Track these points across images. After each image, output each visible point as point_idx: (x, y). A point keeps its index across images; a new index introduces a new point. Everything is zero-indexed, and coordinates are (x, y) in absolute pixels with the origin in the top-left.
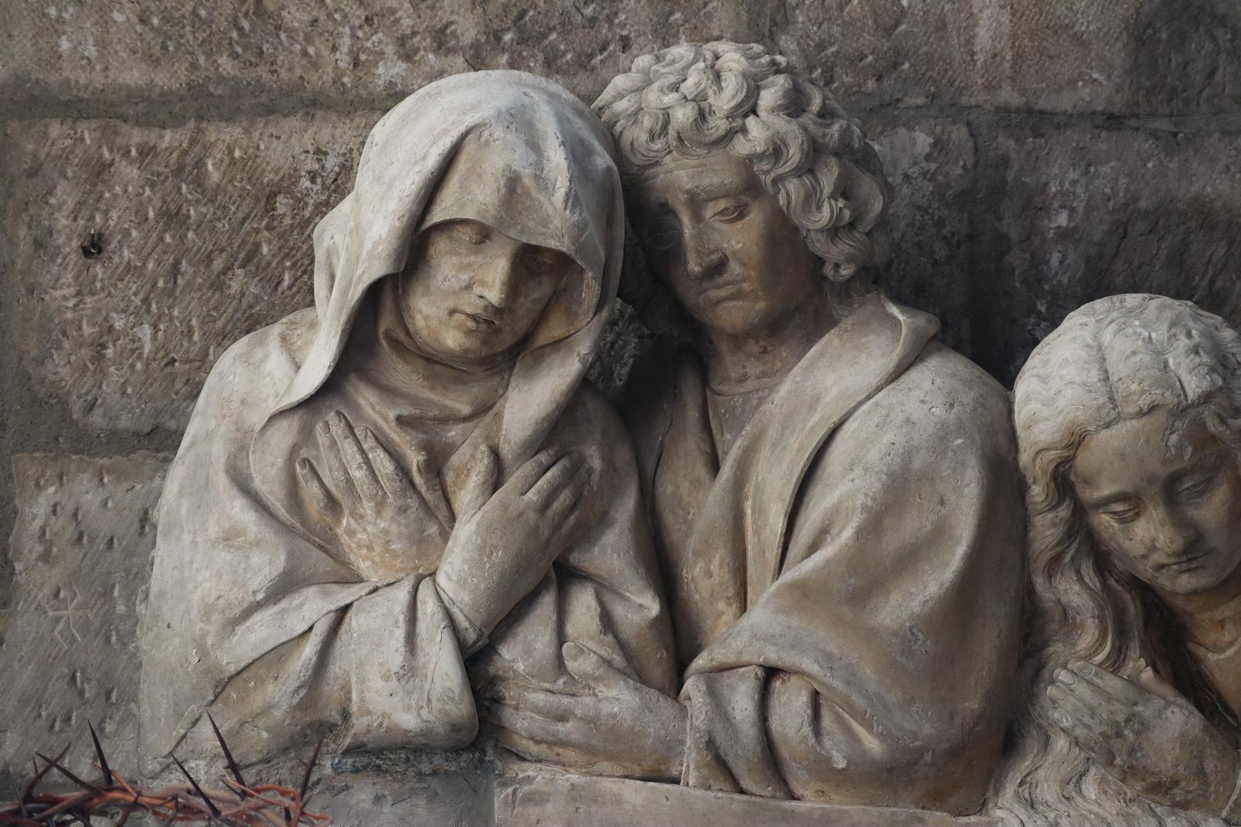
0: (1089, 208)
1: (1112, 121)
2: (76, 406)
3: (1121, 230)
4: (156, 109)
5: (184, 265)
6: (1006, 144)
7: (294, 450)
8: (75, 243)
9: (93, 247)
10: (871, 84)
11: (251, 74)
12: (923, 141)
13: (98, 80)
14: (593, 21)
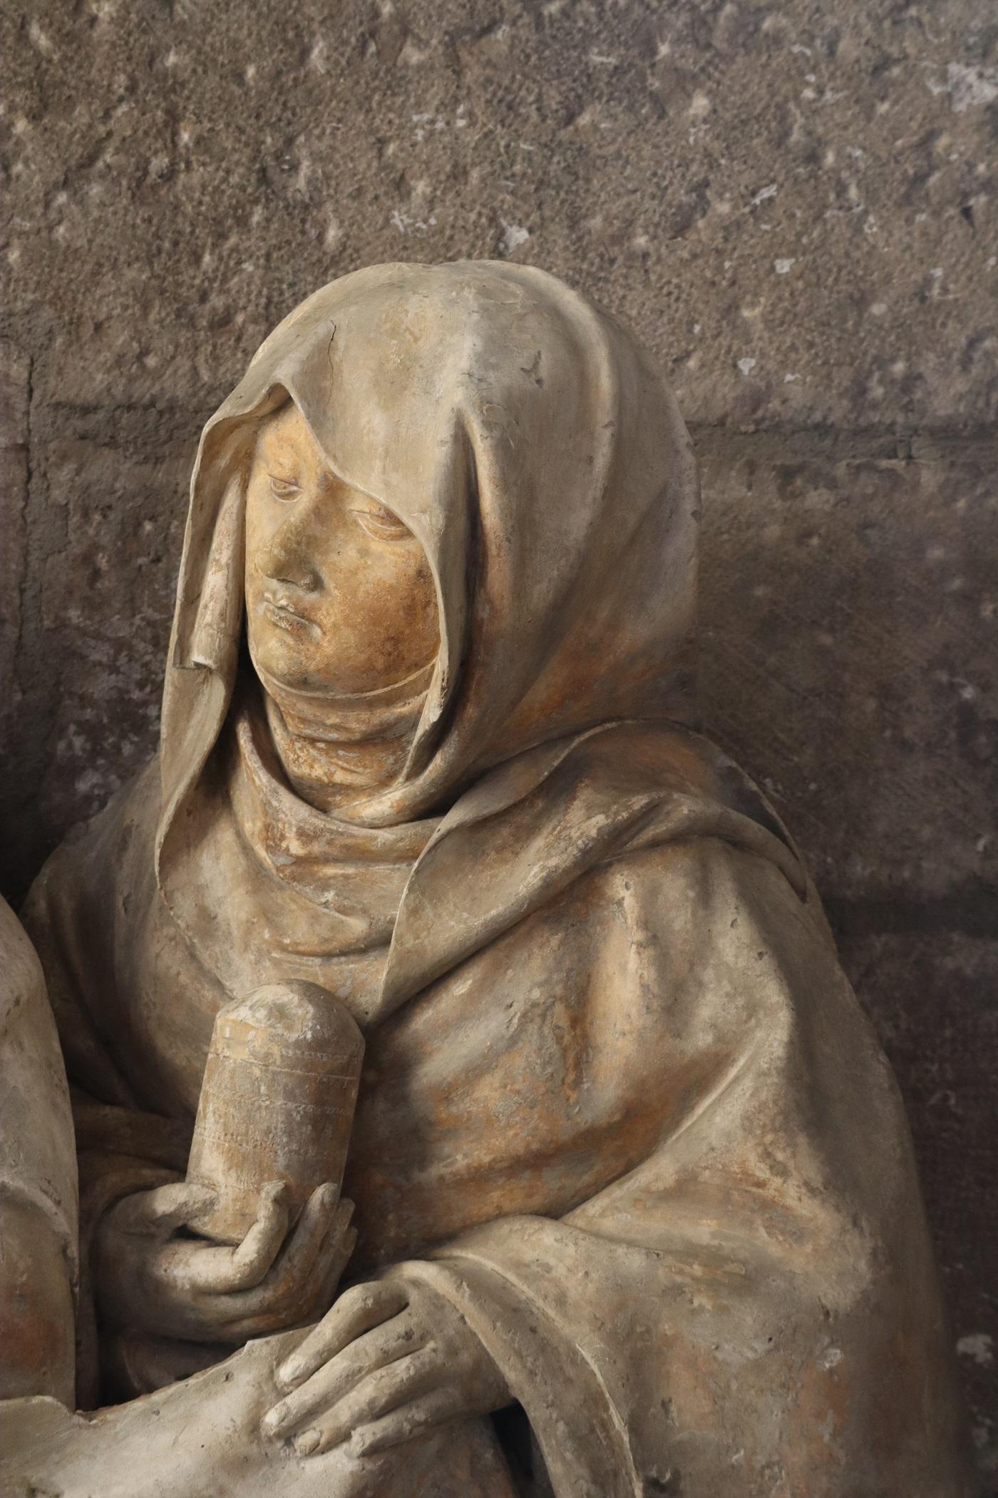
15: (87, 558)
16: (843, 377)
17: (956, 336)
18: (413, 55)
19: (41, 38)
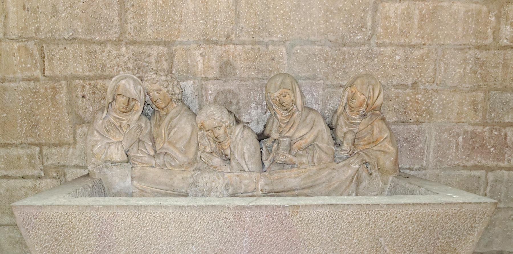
2: (83, 117)
3: (218, 93)
4: (90, 79)
6: (203, 82)
12: (192, 82)
19: (325, 55)
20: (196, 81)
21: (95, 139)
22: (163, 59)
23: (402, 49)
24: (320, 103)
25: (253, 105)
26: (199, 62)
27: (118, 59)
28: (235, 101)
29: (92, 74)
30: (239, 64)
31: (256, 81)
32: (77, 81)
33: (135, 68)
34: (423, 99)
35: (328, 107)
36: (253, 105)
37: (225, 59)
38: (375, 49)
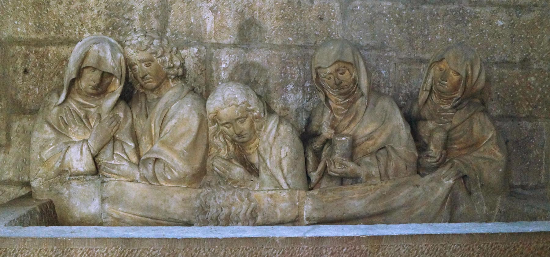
0: (230, 63)
1: (235, 46)
3: (236, 68)
4: (38, 43)
5: (44, 76)
7: (58, 114)
8: (22, 71)
9: (26, 71)
10: (185, 38)
11: (58, 36)
12: (196, 50)
13: (26, 37)
14: (128, 25)
15: (402, 77)
16: (485, 57)
17: (498, 52)
18: (439, 18)
20: (203, 48)
21: (46, 136)
22: (152, 14)
23: (504, 10)
24: (391, 85)
25: (290, 87)
26: (207, 21)
27: (82, 15)
28: (262, 80)
29: (41, 36)
30: (270, 24)
31: (294, 51)
32: (17, 47)
33: (108, 28)
34: (537, 84)
35: (404, 92)
36: (290, 87)
37: (247, 17)
38: (468, 9)
